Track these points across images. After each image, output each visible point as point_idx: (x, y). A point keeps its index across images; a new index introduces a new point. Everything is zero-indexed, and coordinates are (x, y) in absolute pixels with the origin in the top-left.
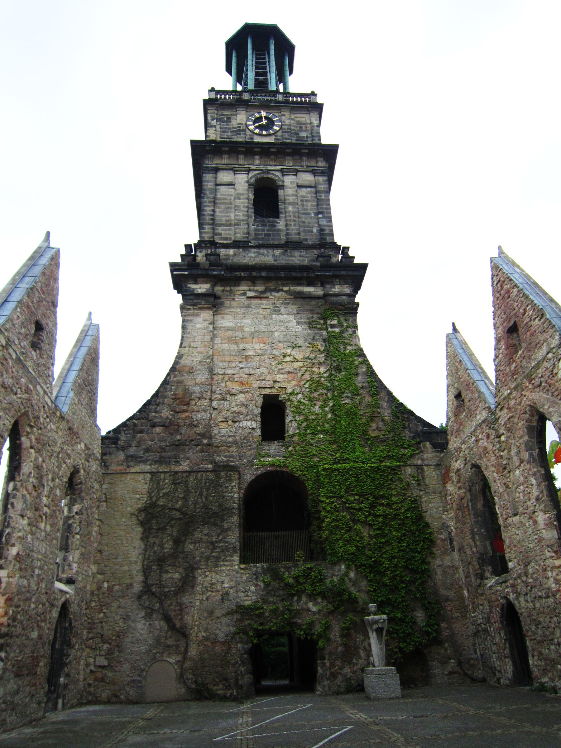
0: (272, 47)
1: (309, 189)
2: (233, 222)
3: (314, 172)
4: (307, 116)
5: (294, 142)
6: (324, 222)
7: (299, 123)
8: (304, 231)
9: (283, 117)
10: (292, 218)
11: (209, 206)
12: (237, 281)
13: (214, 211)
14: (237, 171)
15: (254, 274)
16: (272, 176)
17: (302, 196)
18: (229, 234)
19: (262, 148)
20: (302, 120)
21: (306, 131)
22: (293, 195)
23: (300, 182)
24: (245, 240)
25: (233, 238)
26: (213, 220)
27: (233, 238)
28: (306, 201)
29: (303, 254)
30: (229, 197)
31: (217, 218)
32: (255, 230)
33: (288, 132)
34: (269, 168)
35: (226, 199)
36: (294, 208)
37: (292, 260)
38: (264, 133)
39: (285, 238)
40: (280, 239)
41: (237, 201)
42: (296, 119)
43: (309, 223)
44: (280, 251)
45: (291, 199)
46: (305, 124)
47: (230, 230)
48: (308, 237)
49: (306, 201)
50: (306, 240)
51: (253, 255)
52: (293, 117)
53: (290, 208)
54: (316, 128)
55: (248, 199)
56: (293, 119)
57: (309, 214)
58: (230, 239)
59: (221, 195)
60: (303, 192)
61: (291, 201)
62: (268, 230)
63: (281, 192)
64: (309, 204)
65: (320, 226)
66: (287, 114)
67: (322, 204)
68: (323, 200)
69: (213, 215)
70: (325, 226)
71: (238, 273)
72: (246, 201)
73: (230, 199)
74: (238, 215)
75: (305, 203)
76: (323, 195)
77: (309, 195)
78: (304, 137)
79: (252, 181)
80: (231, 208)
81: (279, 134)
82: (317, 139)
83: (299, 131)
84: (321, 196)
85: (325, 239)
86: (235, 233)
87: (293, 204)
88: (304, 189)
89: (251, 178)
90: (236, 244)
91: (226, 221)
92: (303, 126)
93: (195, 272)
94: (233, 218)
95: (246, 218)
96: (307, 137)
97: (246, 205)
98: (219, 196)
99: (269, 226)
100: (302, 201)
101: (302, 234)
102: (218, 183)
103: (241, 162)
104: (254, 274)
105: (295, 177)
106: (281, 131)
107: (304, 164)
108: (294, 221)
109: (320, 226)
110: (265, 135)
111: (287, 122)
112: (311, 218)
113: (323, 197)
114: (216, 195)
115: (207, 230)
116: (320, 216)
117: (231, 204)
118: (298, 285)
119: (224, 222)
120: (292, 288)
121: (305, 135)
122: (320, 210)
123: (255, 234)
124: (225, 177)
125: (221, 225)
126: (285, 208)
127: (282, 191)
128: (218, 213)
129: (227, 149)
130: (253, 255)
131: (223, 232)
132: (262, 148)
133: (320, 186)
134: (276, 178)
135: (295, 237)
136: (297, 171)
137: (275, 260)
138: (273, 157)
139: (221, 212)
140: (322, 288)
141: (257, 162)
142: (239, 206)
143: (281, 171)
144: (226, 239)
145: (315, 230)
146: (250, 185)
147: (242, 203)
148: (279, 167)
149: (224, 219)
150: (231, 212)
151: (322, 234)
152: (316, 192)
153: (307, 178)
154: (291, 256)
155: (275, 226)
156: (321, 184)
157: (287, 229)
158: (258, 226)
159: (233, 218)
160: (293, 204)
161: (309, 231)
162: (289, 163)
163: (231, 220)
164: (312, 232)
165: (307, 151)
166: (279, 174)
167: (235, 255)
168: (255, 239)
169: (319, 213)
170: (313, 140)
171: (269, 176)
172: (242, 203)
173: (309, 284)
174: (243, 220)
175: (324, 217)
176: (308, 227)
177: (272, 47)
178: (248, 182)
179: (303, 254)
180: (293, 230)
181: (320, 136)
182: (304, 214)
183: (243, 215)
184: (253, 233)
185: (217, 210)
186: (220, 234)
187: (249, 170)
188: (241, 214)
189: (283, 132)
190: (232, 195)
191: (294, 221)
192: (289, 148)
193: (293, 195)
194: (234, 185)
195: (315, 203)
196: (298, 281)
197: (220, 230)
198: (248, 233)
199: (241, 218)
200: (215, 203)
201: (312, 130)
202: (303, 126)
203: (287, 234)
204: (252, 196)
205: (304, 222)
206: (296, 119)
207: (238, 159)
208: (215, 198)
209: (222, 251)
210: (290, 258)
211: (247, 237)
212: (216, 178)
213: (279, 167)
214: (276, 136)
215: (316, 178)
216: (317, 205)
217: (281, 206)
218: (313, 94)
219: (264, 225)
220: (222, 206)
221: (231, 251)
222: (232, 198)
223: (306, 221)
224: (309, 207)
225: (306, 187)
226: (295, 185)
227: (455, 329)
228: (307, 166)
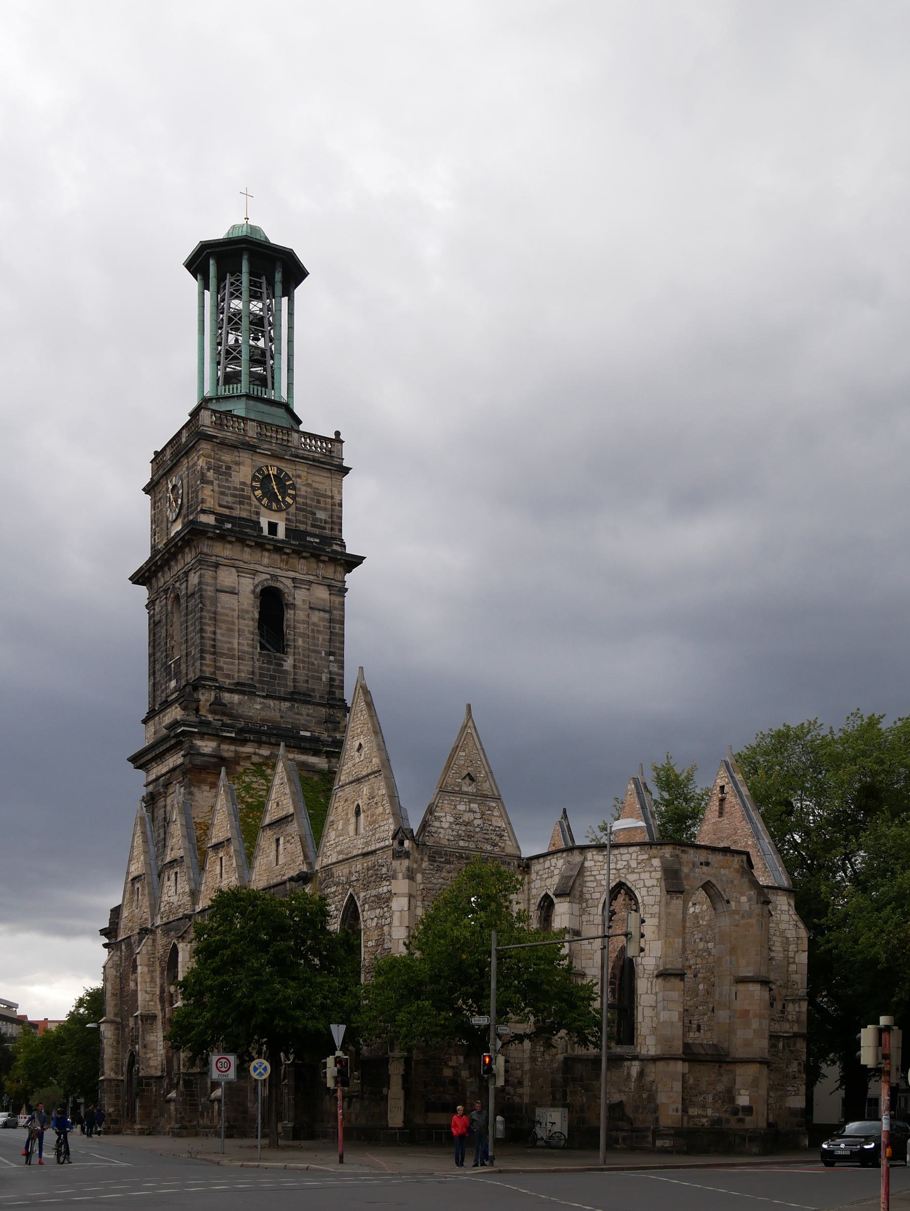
1: (322, 614)
2: (236, 653)
4: (328, 481)
5: (309, 529)
6: (334, 668)
7: (317, 493)
8: (313, 677)
9: (299, 480)
10: (301, 657)
11: (209, 625)
12: (244, 742)
13: (215, 633)
14: (242, 572)
15: (264, 738)
16: (281, 586)
17: (314, 624)
18: (232, 670)
19: (275, 546)
20: (320, 487)
21: (325, 510)
22: (304, 622)
24: (250, 682)
25: (236, 676)
26: (214, 646)
27: (236, 676)
28: (318, 631)
29: (311, 711)
30: (231, 613)
31: (218, 644)
32: (261, 668)
34: (279, 572)
35: (227, 615)
36: (304, 642)
37: (299, 719)
38: (274, 506)
39: (292, 684)
40: (286, 686)
41: (241, 621)
43: (318, 666)
44: (288, 704)
45: (301, 628)
46: (326, 496)
47: (232, 664)
50: (313, 690)
51: (258, 707)
53: (300, 642)
54: (337, 508)
55: (253, 620)
56: (309, 485)
58: (233, 679)
59: (223, 608)
60: (316, 617)
61: (302, 631)
62: (274, 671)
63: (289, 614)
65: (330, 673)
66: (304, 474)
69: (214, 640)
71: (247, 735)
72: (251, 623)
73: (233, 616)
74: (243, 645)
75: (316, 635)
76: (337, 626)
77: (322, 624)
78: (321, 520)
79: (258, 590)
80: (232, 630)
81: (292, 510)
82: (337, 527)
83: (316, 508)
84: (334, 628)
85: (334, 693)
86: (239, 672)
87: (303, 635)
88: (317, 612)
89: (257, 585)
90: (239, 688)
91: (229, 649)
92: (322, 499)
93: (204, 730)
94: (236, 646)
95: (251, 650)
96: (326, 522)
97: (251, 629)
98: (219, 609)
99: (277, 664)
100: (313, 631)
101: (310, 681)
102: (218, 588)
103: (246, 557)
104: (264, 738)
105: (307, 593)
106: (294, 506)
107: (321, 572)
108: (304, 662)
109: (330, 673)
110: (275, 511)
111: (303, 488)
112: (321, 658)
114: (217, 607)
115: (207, 662)
116: (332, 658)
117: (233, 623)
118: (303, 753)
119: (225, 652)
120: (297, 756)
121: (323, 518)
122: (332, 650)
123: (261, 675)
124: (227, 577)
125: (223, 655)
126: (294, 640)
127: (292, 612)
128: (219, 637)
129: (233, 539)
130: (258, 707)
131: (225, 666)
132: (275, 546)
133: (335, 612)
134: (286, 590)
135: (302, 686)
137: (282, 717)
138: (284, 557)
139: (223, 635)
140: (326, 760)
141: (266, 561)
142: (244, 630)
143: (294, 580)
144: (228, 676)
146: (256, 597)
147: (247, 626)
148: (292, 574)
149: (226, 646)
150: (234, 638)
151: (331, 686)
153: (321, 594)
154: (297, 714)
155: (282, 665)
157: (295, 674)
158: (263, 663)
159: (236, 646)
160: (303, 635)
162: (302, 569)
163: (233, 649)
166: (289, 583)
167: (240, 703)
168: (261, 682)
170: (332, 529)
171: (278, 585)
172: (247, 626)
173: (316, 753)
174: (247, 653)
175: (336, 661)
176: (317, 672)
178: (253, 592)
179: (311, 711)
180: (302, 675)
181: (341, 524)
182: (314, 651)
183: (248, 645)
184: (257, 671)
185: (218, 631)
186: (221, 669)
187: (255, 573)
188: (245, 642)
189: (297, 509)
190: (234, 610)
191: (304, 662)
193: (304, 622)
194: (237, 594)
195: (327, 637)
196: (304, 751)
197: (222, 662)
198: (253, 673)
199: (246, 648)
200: (215, 619)
201: (333, 510)
202: (322, 499)
203: (294, 680)
204: (257, 616)
205: (313, 664)
206: (315, 485)
207: (242, 551)
208: (215, 613)
209: (226, 697)
210: (297, 717)
211: (252, 679)
212: (216, 578)
213: (292, 574)
214: (288, 514)
216: (330, 640)
217: (289, 634)
218: (338, 439)
219: (269, 663)
220: (224, 626)
221: (236, 698)
222: (236, 614)
223: (316, 662)
224: (321, 641)
225: (320, 610)
226: (307, 607)
228: (323, 578)
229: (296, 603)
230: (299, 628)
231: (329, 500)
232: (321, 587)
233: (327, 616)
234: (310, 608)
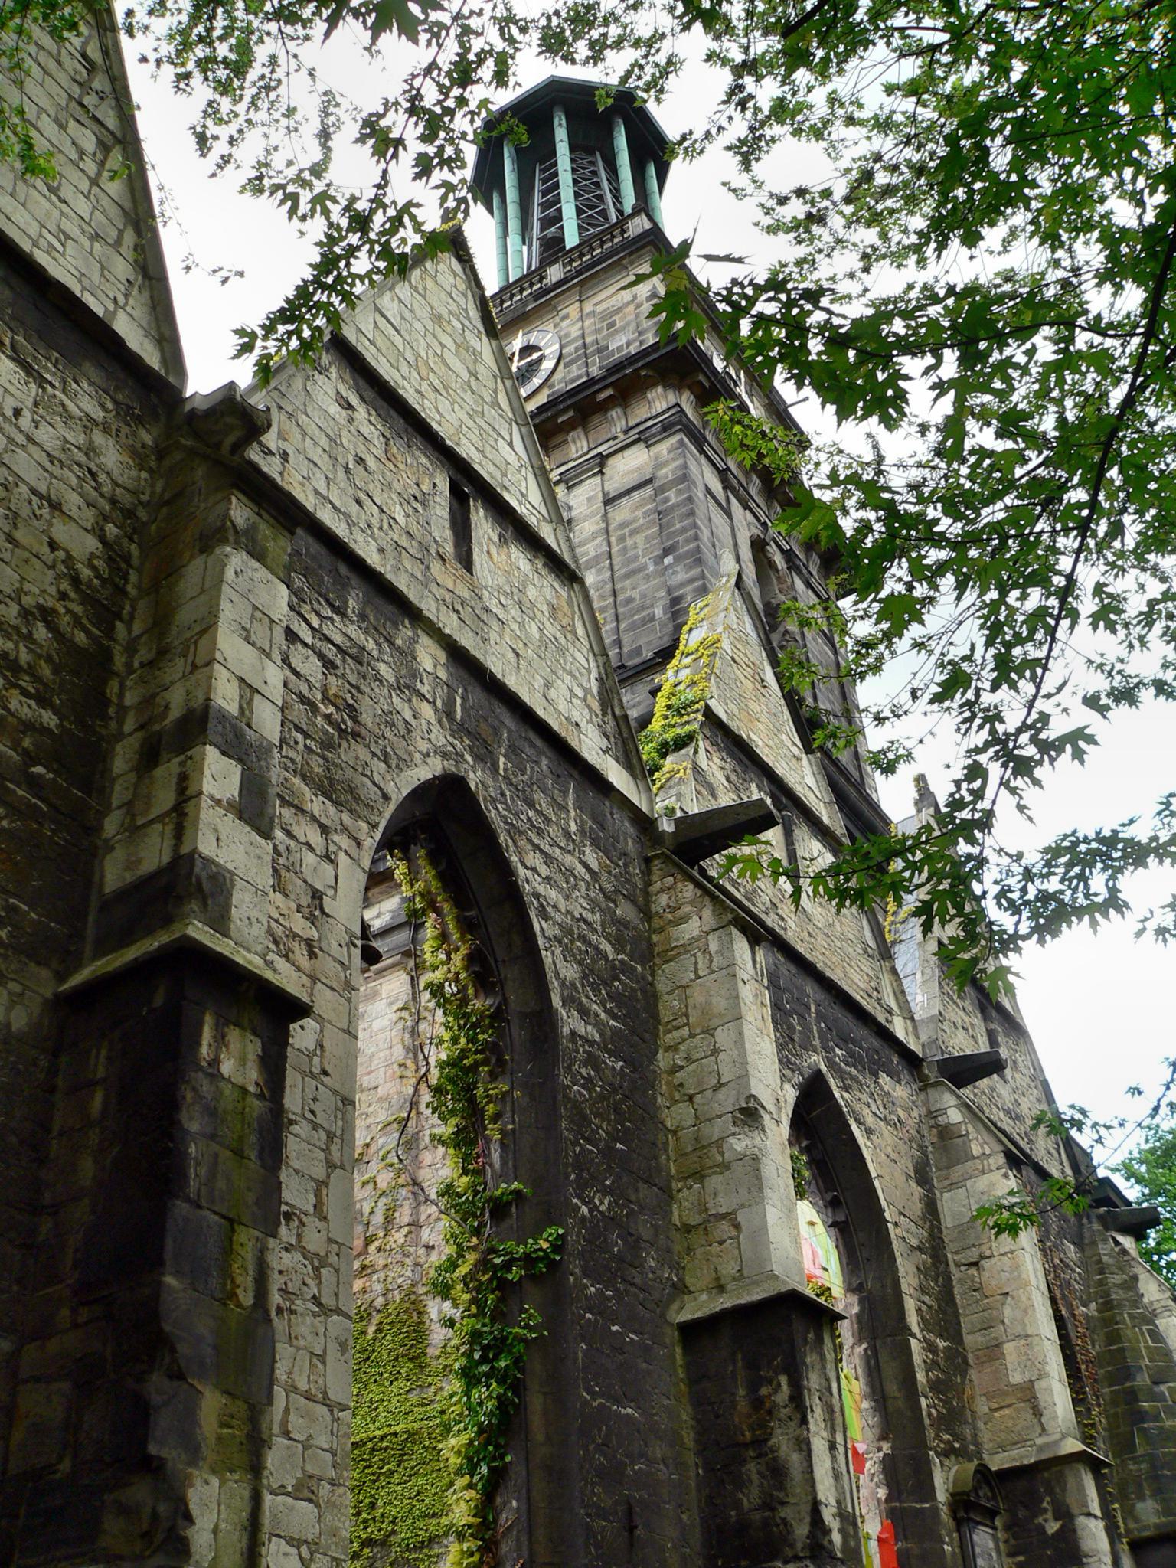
0: (561, 134)
1: (636, 496)
3: (644, 437)
17: (622, 526)
23: (614, 485)
33: (578, 358)
36: (599, 572)
42: (600, 308)
43: (643, 596)
48: (642, 642)
49: (632, 533)
52: (588, 307)
57: (644, 568)
60: (622, 512)
61: (592, 554)
64: (639, 539)
65: (669, 591)
67: (669, 525)
68: (672, 507)
70: (682, 585)
83: (610, 336)
88: (625, 500)
92: (616, 318)
100: (622, 539)
101: (626, 639)
105: (597, 480)
113: (673, 501)
116: (668, 560)
136: (602, 460)
145: (659, 612)
152: (658, 492)
156: (666, 464)
161: (644, 621)
164: (652, 619)
165: (609, 392)
169: (667, 552)
175: (677, 560)
176: (643, 608)
177: (561, 134)
182: (627, 576)
192: (565, 410)
205: (630, 600)
206: (600, 308)
215: (654, 450)
223: (635, 594)
225: (628, 492)
227: (1030, 819)
229: (574, 513)
230: (585, 554)
231: (632, 307)
232: (627, 453)
233: (648, 491)
234: (609, 501)
